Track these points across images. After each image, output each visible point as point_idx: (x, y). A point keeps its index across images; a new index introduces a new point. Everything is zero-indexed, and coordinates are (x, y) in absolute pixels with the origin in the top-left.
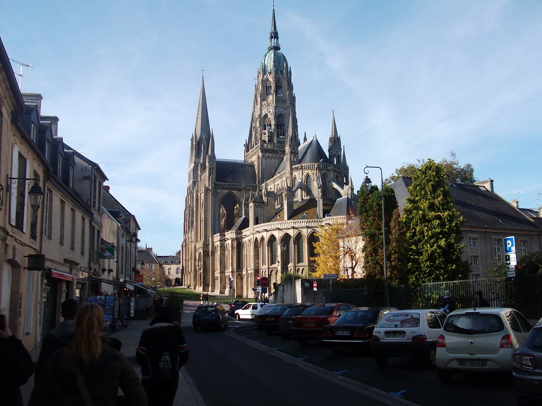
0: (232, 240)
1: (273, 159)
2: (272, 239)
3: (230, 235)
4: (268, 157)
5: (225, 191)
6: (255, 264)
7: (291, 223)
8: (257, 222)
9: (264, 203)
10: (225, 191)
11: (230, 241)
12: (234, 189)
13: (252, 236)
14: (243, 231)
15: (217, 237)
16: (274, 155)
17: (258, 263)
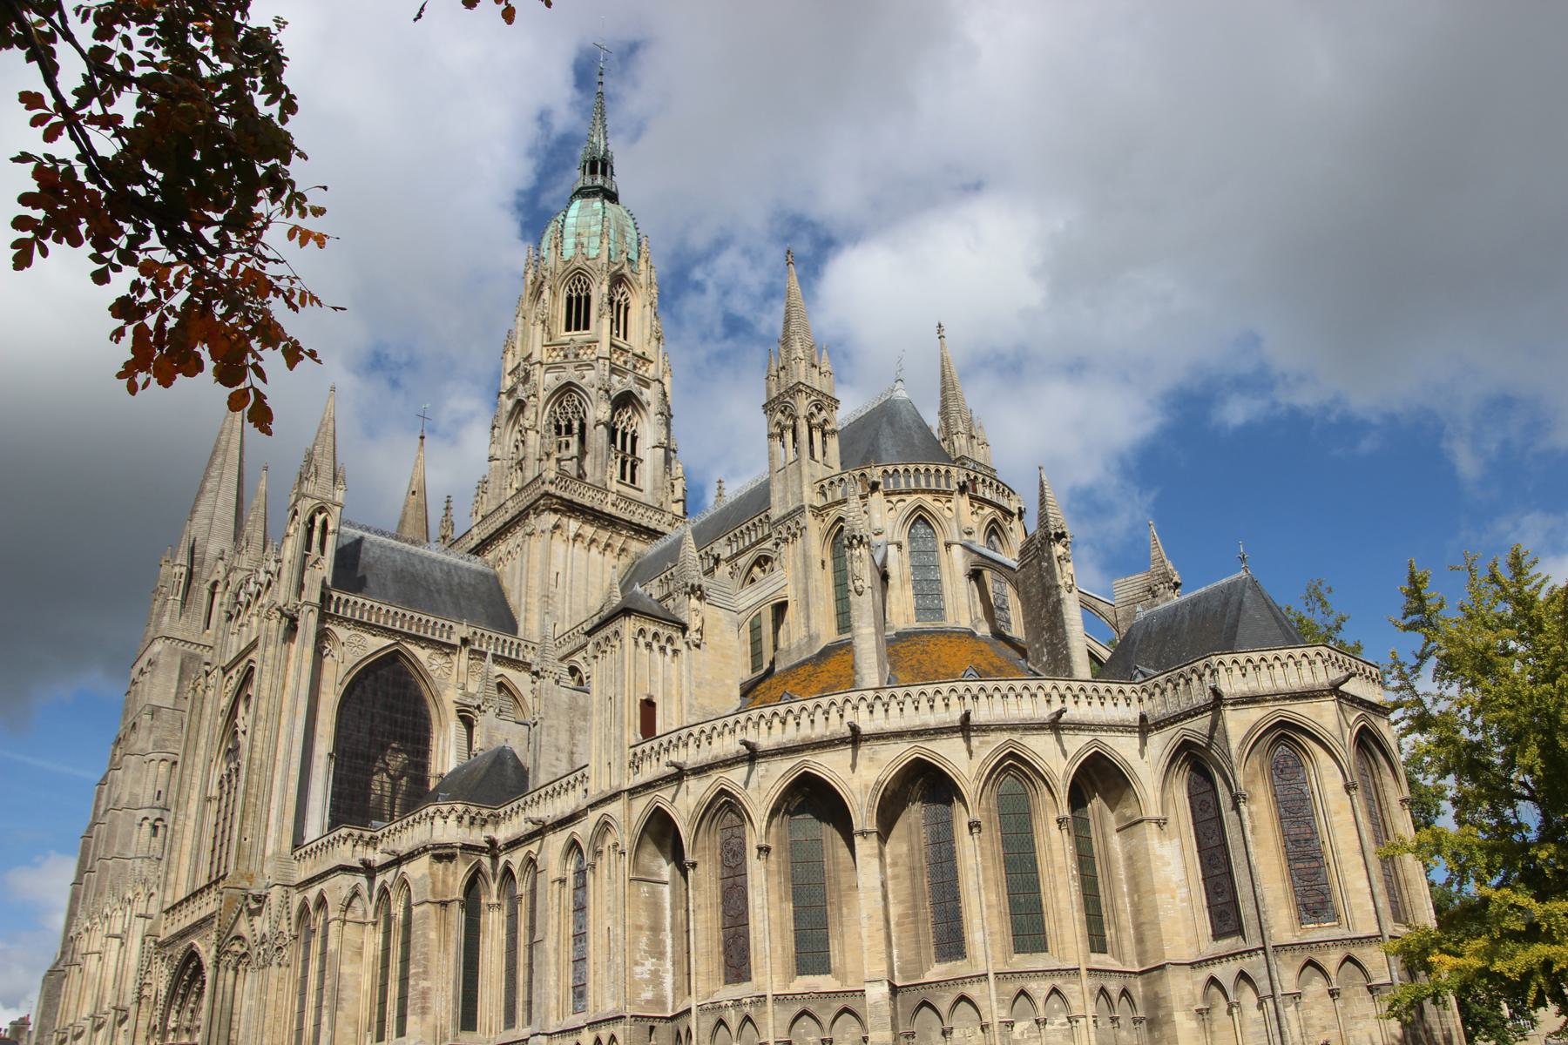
0: (438, 858)
4: (578, 535)
5: (376, 643)
12: (417, 639)
13: (615, 809)
14: (502, 811)
16: (604, 536)
17: (656, 978)
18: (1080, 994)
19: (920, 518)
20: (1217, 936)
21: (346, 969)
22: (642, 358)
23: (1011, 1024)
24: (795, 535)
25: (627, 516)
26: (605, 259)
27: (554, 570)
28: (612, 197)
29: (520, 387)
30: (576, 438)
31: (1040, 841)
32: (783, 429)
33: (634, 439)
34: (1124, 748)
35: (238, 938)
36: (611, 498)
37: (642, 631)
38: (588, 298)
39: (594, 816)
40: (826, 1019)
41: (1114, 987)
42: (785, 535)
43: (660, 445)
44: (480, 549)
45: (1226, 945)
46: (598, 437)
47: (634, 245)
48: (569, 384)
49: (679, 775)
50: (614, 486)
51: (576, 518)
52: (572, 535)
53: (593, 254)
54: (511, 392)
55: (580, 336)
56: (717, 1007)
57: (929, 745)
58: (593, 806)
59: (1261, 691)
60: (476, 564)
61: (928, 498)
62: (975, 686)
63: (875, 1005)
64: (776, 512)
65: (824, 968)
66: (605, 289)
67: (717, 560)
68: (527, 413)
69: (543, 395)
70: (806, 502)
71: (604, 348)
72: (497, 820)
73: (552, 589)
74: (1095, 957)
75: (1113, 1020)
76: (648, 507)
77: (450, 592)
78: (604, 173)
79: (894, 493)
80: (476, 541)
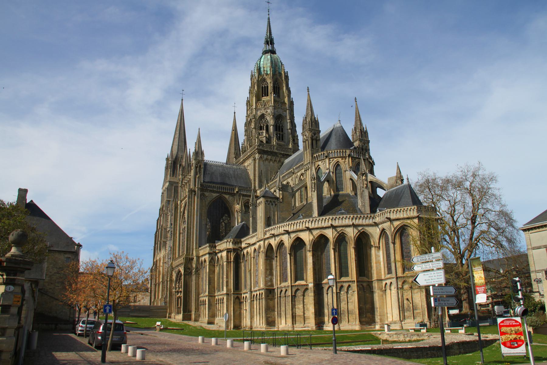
0: (228, 252)
1: (271, 162)
2: (298, 244)
3: (224, 245)
5: (215, 195)
6: (266, 282)
7: (327, 221)
8: (268, 223)
9: (278, 198)
10: (215, 195)
11: (224, 254)
12: (225, 193)
13: (262, 242)
15: (205, 250)
16: (274, 158)
17: (271, 280)
18: (354, 286)
19: (337, 165)
20: (388, 273)
21: (211, 276)
23: (340, 293)
30: (264, 131)
31: (349, 252)
34: (370, 230)
35: (189, 269)
37: (267, 201)
38: (267, 87)
39: (258, 244)
40: (303, 290)
41: (365, 284)
45: (389, 276)
48: (263, 114)
49: (274, 236)
56: (281, 287)
57: (324, 231)
58: (258, 242)
59: (400, 217)
61: (340, 159)
62: (334, 217)
63: (311, 288)
65: (303, 279)
72: (241, 242)
74: (361, 278)
75: (364, 292)
77: (235, 177)
78: (271, 44)
79: (331, 158)
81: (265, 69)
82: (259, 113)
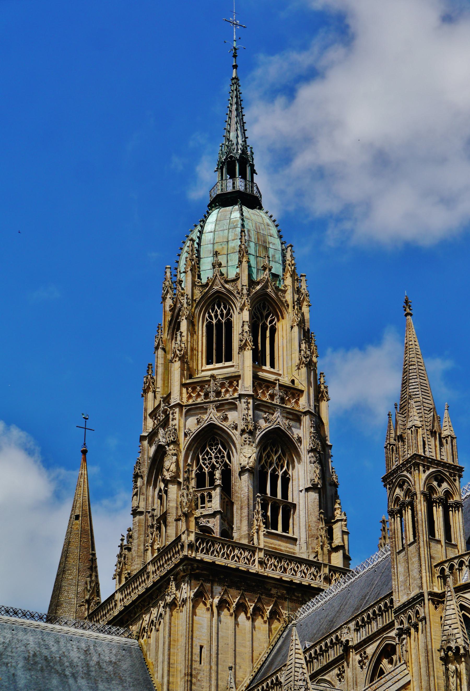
22: (292, 392)
24: (416, 627)
25: (276, 574)
26: (245, 280)
27: (197, 644)
28: (252, 201)
29: (161, 431)
32: (403, 506)
33: (286, 481)
36: (260, 555)
38: (229, 324)
42: (406, 625)
43: (313, 488)
44: (124, 620)
46: (243, 486)
47: (279, 256)
50: (262, 541)
51: (220, 583)
52: (216, 601)
53: (232, 276)
54: (153, 436)
55: (220, 370)
60: (118, 639)
64: (400, 599)
66: (246, 315)
67: (347, 648)
68: (167, 464)
69: (184, 443)
70: (425, 590)
71: (246, 385)
73: (196, 665)
76: (301, 561)
77: (88, 674)
80: (120, 607)
81: (222, 259)
82: (192, 424)
